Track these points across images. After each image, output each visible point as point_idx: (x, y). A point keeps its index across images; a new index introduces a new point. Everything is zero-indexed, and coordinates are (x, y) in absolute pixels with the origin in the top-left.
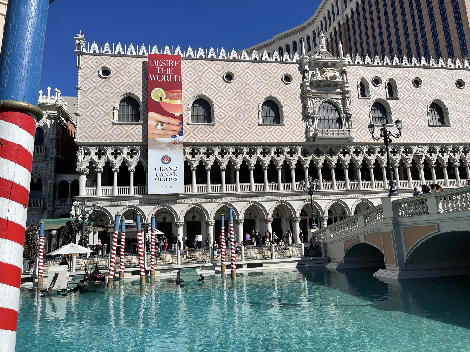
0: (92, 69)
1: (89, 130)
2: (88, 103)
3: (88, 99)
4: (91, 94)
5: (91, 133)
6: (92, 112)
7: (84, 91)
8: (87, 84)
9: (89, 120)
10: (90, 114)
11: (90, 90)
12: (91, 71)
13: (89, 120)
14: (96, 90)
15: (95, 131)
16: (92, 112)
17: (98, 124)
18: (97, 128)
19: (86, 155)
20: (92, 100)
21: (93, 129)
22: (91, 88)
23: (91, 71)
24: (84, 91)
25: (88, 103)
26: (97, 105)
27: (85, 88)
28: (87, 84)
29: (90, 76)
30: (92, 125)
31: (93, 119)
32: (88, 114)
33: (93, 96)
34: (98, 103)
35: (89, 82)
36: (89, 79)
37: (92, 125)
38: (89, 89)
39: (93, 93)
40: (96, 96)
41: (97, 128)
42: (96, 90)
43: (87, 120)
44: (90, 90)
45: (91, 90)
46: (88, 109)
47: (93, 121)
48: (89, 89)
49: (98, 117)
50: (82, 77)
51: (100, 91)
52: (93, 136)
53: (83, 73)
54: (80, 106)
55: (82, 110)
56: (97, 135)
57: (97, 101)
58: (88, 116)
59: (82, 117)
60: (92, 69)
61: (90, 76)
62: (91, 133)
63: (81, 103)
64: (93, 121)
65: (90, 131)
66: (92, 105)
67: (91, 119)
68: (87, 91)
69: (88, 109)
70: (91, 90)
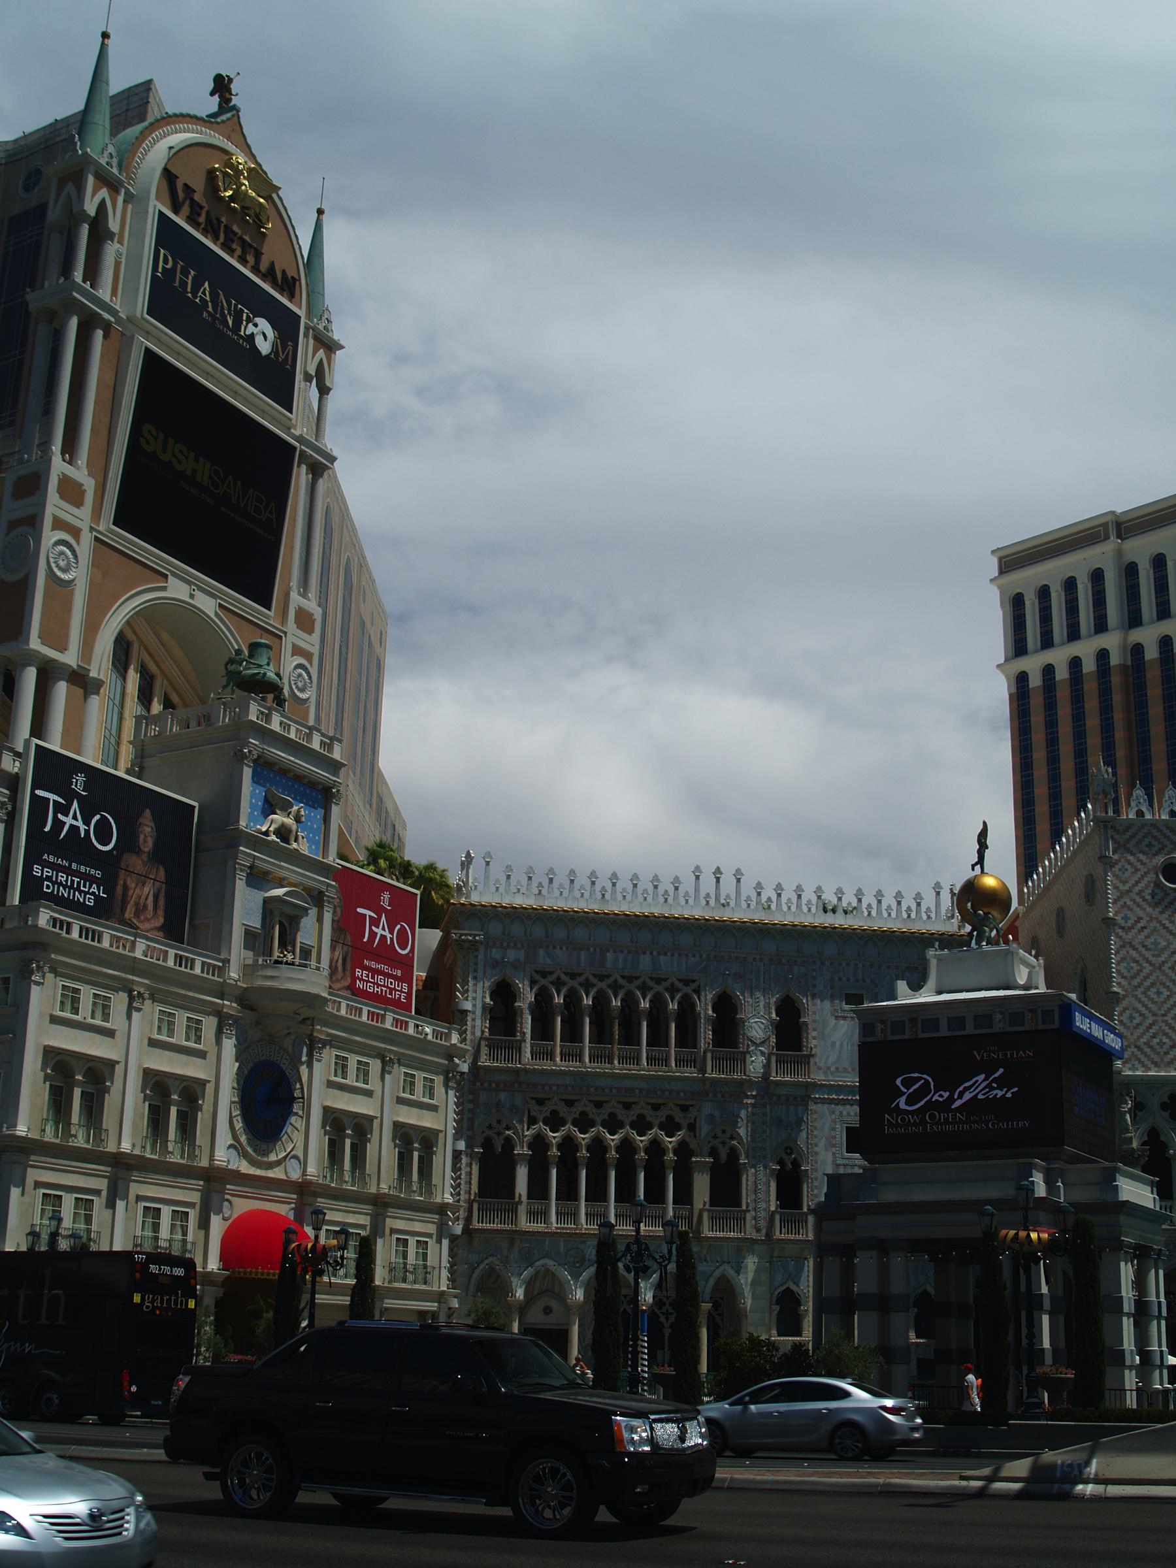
0: (1139, 866)
1: (1144, 1040)
2: (1136, 961)
3: (1135, 949)
4: (1142, 937)
5: (1151, 1047)
6: (1148, 989)
7: (1123, 928)
8: (1129, 909)
9: (1143, 1010)
10: (1145, 993)
11: (1139, 925)
12: (1137, 870)
13: (1143, 1010)
14: (1154, 924)
15: (1161, 1044)
16: (1148, 989)
17: (1166, 1022)
18: (1166, 1034)
19: (1141, 1111)
20: (1148, 954)
21: (1154, 1037)
22: (1140, 919)
23: (1137, 870)
24: (1123, 928)
25: (1136, 961)
26: (1160, 968)
27: (1126, 918)
28: (1129, 909)
29: (1137, 883)
30: (1150, 1026)
31: (1153, 1007)
32: (1139, 993)
33: (1149, 942)
34: (1163, 963)
35: (1134, 901)
36: (1133, 895)
37: (1150, 1026)
38: (1136, 922)
39: (1146, 932)
40: (1156, 943)
41: (1166, 1034)
42: (1154, 924)
43: (1137, 1011)
44: (1139, 925)
45: (1141, 924)
46: (1138, 980)
47: (1155, 1015)
48: (1136, 922)
49: (1165, 1002)
50: (1115, 887)
51: (1165, 927)
52: (1156, 1059)
53: (1117, 876)
54: (1118, 972)
55: (1124, 983)
56: (1167, 1053)
57: (1158, 956)
58: (1140, 1001)
59: (1124, 1004)
60: (1139, 866)
61: (1137, 883)
62: (1151, 1047)
63: (1118, 964)
64: (1155, 1015)
65: (1147, 1044)
66: (1148, 968)
67: (1147, 1008)
68: (1132, 928)
69: (1138, 980)
70: (1141, 924)
